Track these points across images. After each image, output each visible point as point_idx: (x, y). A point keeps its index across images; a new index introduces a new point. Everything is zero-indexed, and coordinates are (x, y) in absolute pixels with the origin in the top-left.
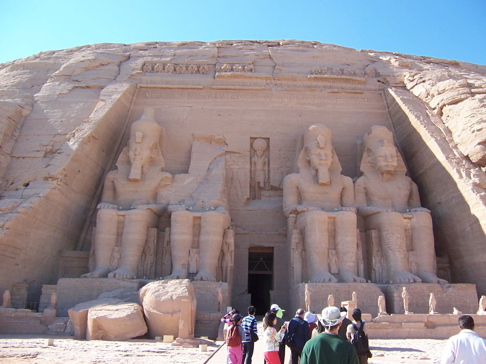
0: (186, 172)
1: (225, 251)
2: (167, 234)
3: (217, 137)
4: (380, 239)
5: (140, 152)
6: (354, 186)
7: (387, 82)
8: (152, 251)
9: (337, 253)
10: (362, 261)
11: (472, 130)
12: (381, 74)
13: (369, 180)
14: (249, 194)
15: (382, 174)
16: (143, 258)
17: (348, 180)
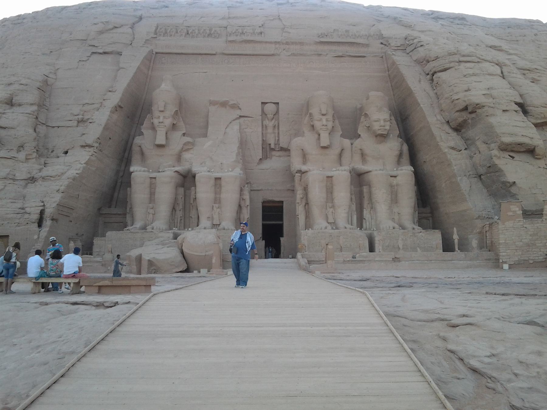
0: (205, 135)
1: (242, 205)
2: (193, 193)
3: (231, 103)
4: (370, 193)
5: (162, 118)
6: (352, 147)
7: (389, 44)
8: (181, 207)
9: (333, 207)
10: (355, 213)
11: (453, 99)
12: (384, 36)
13: (366, 142)
14: (261, 155)
15: (376, 136)
16: (174, 213)
17: (347, 142)
